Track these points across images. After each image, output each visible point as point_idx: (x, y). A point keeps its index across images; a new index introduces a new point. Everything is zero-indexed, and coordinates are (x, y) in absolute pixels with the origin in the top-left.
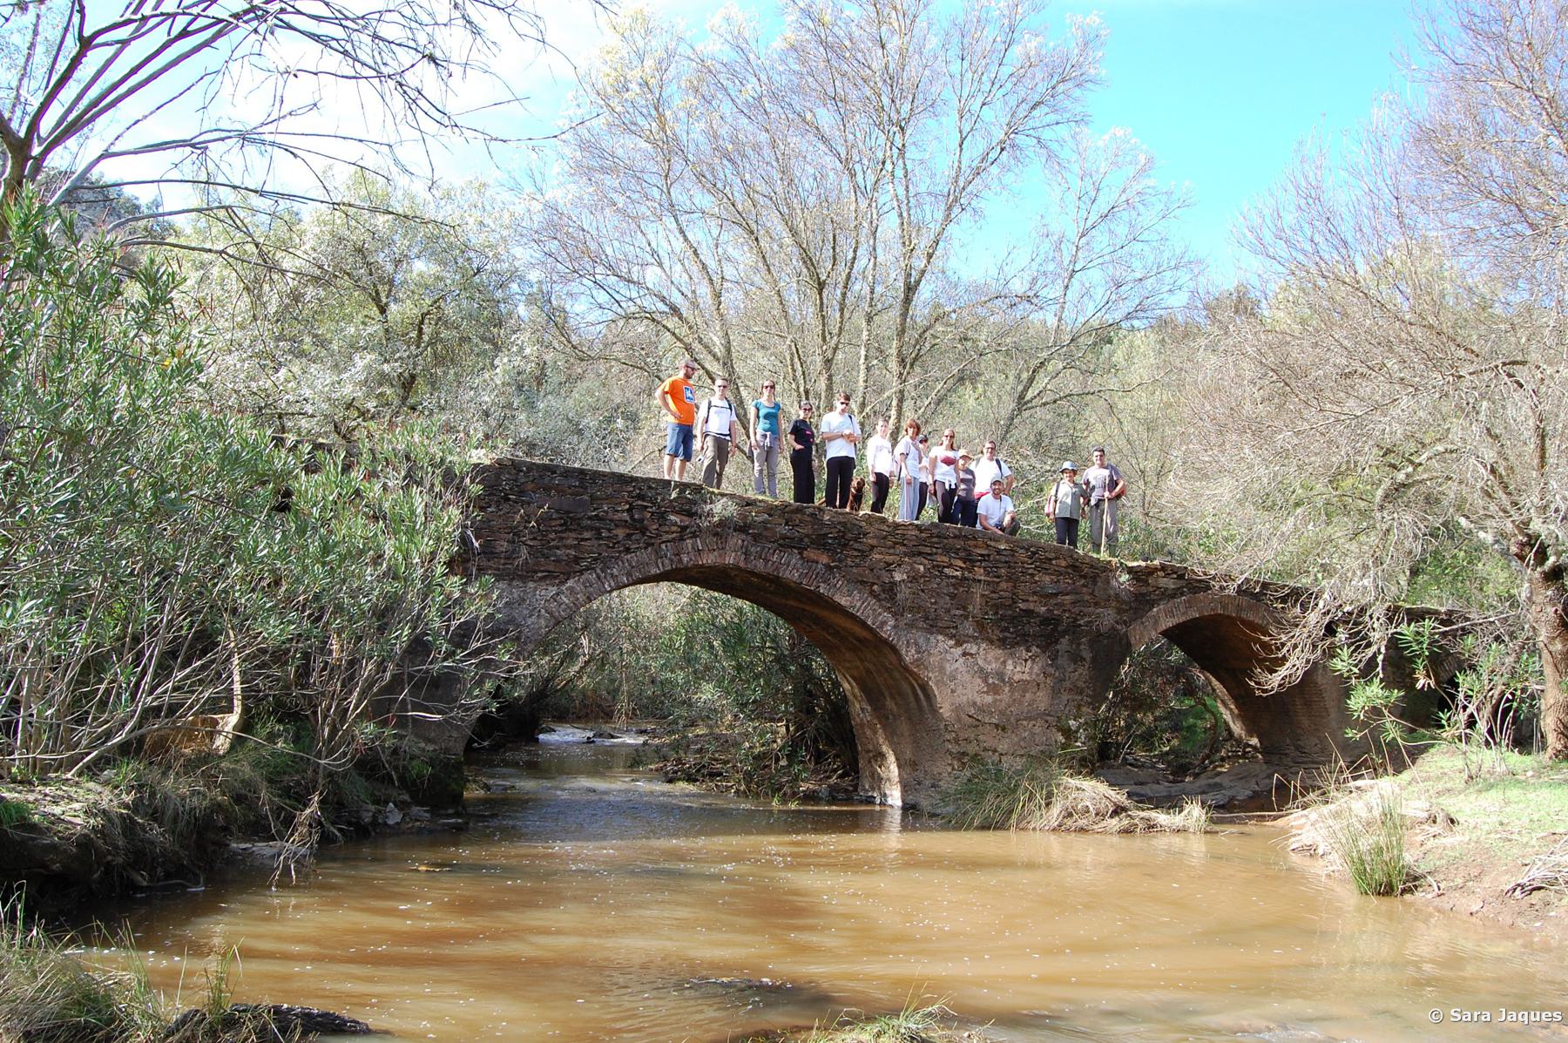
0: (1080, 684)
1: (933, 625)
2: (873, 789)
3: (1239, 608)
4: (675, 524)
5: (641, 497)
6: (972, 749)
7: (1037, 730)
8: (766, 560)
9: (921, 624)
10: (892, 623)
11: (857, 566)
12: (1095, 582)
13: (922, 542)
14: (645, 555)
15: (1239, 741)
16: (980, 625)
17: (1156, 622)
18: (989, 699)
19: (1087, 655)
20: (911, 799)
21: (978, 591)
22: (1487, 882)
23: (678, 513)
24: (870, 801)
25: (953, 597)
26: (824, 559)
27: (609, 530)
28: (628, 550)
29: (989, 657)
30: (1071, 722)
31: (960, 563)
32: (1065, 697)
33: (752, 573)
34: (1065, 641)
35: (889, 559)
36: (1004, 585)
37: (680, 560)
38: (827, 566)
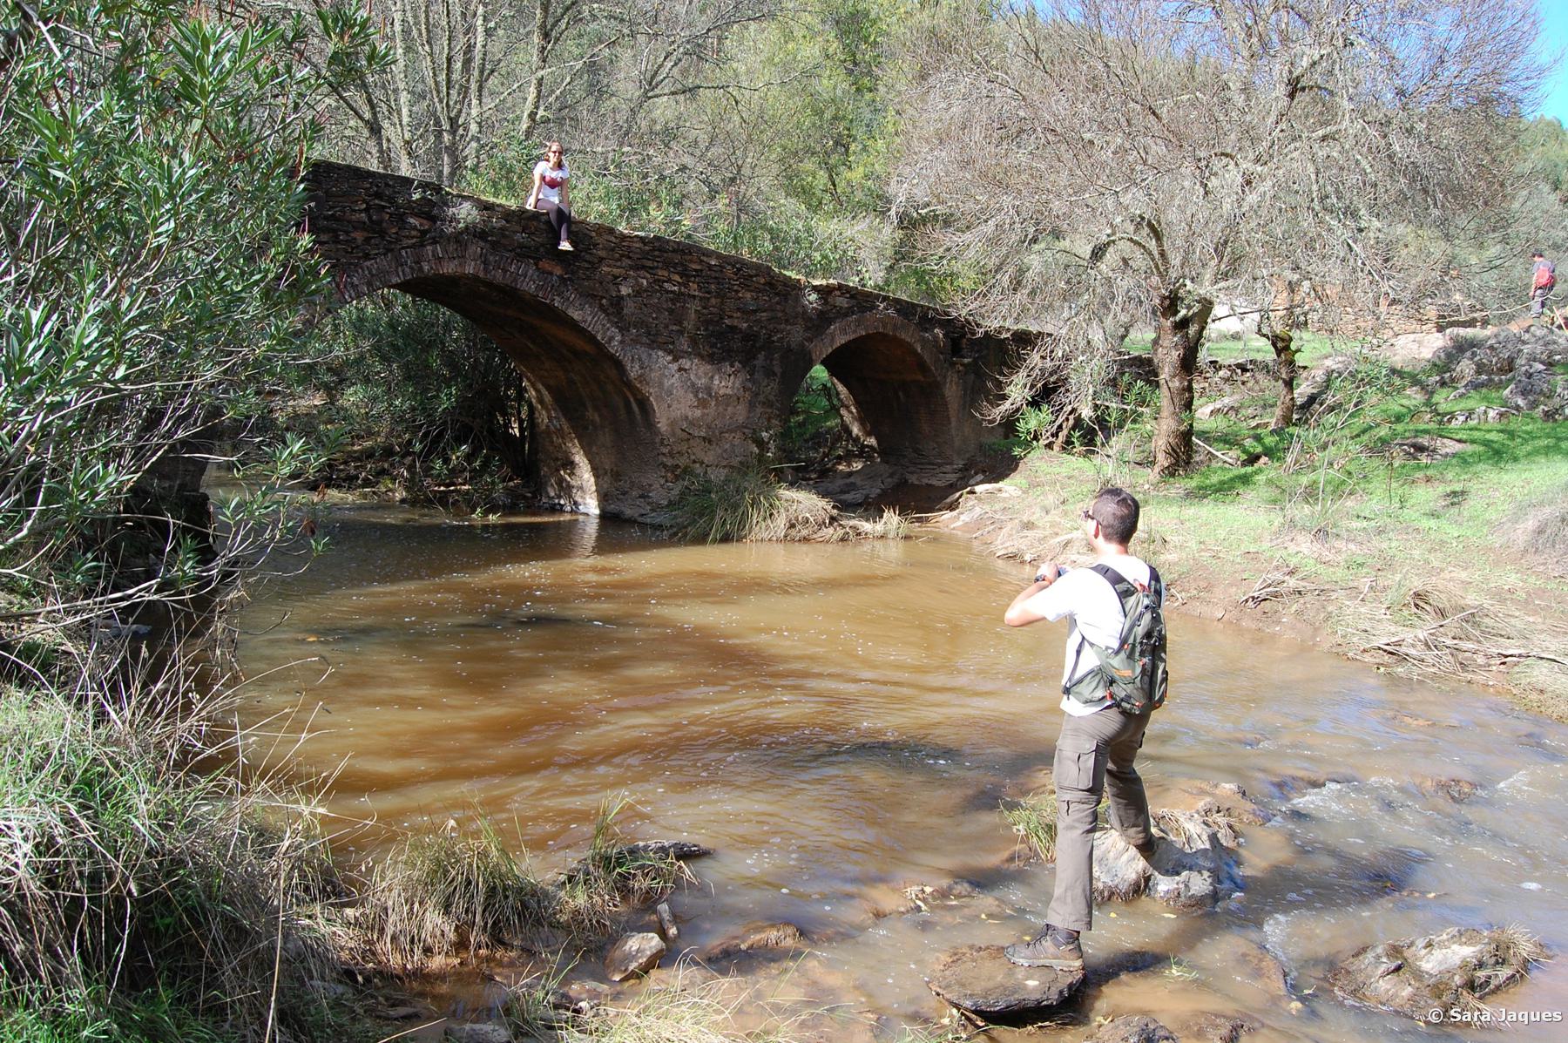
0: (772, 398)
1: (655, 341)
2: (560, 497)
3: (895, 327)
4: (415, 228)
5: (378, 195)
6: (682, 461)
7: (736, 442)
8: (505, 271)
9: (644, 339)
10: (618, 338)
11: (589, 278)
12: (786, 300)
13: (645, 255)
14: (384, 262)
15: (857, 440)
16: (694, 341)
17: (833, 340)
18: (698, 413)
19: (778, 370)
20: (612, 508)
21: (693, 307)
22: (1218, 592)
23: (416, 215)
24: (556, 509)
25: (671, 311)
26: (558, 271)
27: (347, 233)
28: (367, 257)
29: (699, 371)
30: (764, 434)
31: (677, 278)
32: (759, 410)
33: (490, 285)
34: (761, 356)
35: (616, 271)
36: (713, 301)
37: (421, 269)
38: (560, 277)
